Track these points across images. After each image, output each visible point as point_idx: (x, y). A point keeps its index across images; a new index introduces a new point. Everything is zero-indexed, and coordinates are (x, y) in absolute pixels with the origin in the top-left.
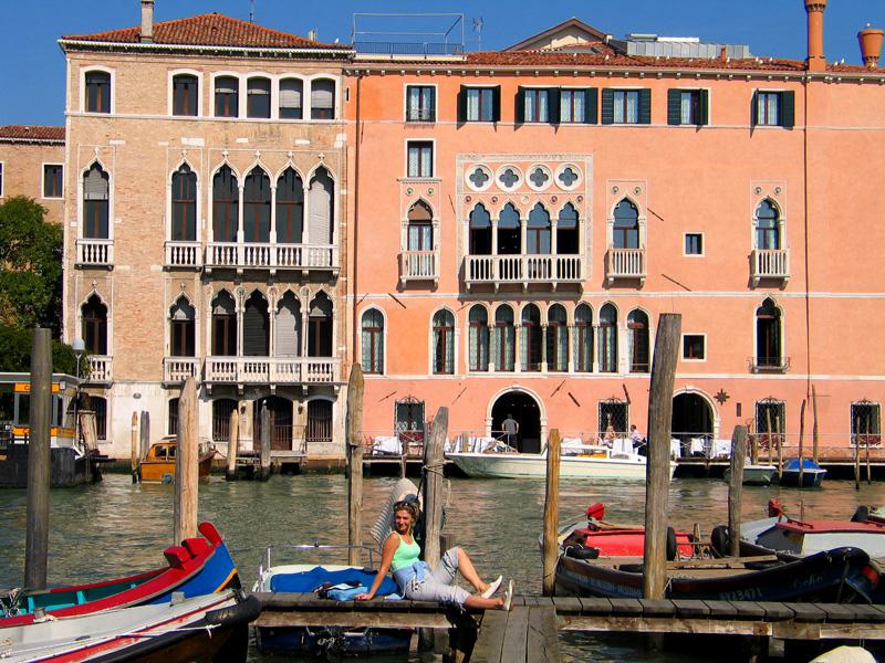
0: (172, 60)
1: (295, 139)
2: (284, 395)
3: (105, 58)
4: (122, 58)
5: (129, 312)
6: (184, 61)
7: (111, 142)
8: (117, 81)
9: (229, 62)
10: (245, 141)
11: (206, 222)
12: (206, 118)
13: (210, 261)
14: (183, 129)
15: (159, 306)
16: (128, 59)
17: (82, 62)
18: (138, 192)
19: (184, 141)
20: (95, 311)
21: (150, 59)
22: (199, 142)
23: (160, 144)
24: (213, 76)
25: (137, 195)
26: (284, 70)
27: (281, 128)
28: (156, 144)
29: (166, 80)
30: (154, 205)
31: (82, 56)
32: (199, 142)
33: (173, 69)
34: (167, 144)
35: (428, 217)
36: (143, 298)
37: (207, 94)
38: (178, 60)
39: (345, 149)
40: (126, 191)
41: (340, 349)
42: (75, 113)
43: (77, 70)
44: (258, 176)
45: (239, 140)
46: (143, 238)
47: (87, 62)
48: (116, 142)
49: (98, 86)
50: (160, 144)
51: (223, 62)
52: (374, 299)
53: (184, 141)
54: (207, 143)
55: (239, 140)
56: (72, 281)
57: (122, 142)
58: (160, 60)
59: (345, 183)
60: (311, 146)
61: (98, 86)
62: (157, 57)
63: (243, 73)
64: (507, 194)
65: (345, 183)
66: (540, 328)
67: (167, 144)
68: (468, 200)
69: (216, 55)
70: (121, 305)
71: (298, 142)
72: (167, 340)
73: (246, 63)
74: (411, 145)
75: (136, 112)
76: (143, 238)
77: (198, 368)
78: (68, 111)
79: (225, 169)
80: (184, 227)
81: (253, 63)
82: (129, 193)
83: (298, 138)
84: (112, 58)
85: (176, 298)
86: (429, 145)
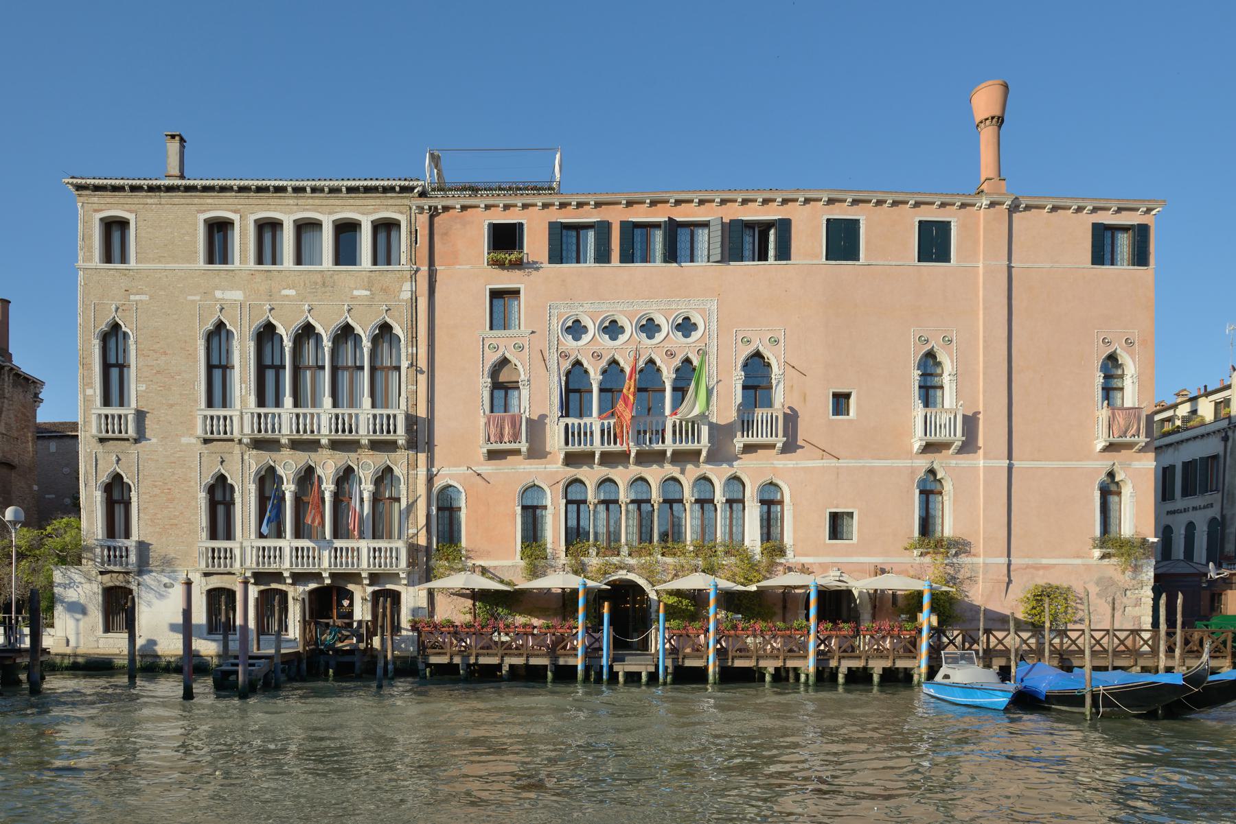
0: (202, 201)
1: (352, 289)
2: (340, 583)
3: (122, 201)
4: (142, 201)
5: (157, 491)
6: (216, 201)
7: (132, 297)
9: (271, 201)
10: (292, 292)
12: (243, 267)
13: (247, 430)
14: (217, 280)
15: (192, 483)
16: (149, 201)
17: (96, 207)
19: (218, 294)
20: (117, 494)
21: (176, 201)
22: (238, 295)
23: (190, 298)
25: (163, 358)
26: (338, 209)
27: (336, 277)
29: (196, 224)
31: (95, 199)
32: (238, 295)
34: (198, 298)
36: (174, 474)
37: (243, 240)
38: (209, 201)
39: (414, 300)
43: (91, 214)
44: (306, 332)
45: (285, 292)
46: (171, 406)
48: (138, 297)
49: (114, 229)
50: (190, 298)
51: (263, 201)
53: (218, 294)
54: (246, 294)
55: (285, 292)
57: (144, 297)
58: (188, 201)
60: (372, 298)
61: (114, 229)
62: (183, 197)
63: (288, 214)
65: (414, 339)
67: (198, 298)
71: (356, 293)
72: (203, 519)
73: (291, 202)
75: (160, 262)
76: (171, 406)
77: (237, 552)
78: (80, 263)
80: (217, 394)
81: (301, 202)
84: (129, 201)
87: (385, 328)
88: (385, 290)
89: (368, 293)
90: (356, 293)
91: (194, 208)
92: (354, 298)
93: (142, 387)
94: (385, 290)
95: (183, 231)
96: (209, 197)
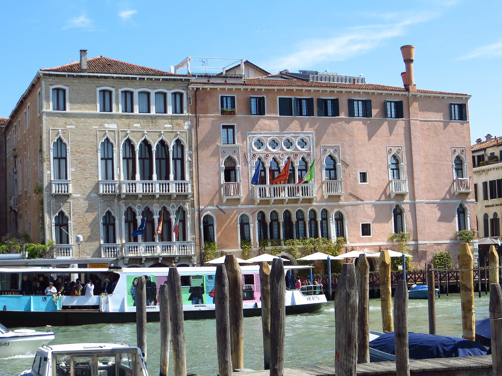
7: (68, 127)
8: (70, 93)
11: (120, 169)
16: (75, 81)
18: (82, 153)
23: (94, 127)
24: (120, 90)
25: (82, 156)
28: (92, 127)
30: (92, 161)
33: (99, 87)
34: (97, 127)
35: (233, 165)
39: (190, 130)
40: (77, 153)
41: (192, 236)
42: (48, 110)
44: (146, 144)
46: (87, 178)
47: (53, 83)
48: (70, 127)
50: (94, 127)
52: (209, 210)
53: (106, 125)
56: (49, 204)
59: (190, 147)
60: (173, 128)
64: (273, 153)
66: (291, 223)
67: (97, 127)
68: (254, 155)
69: (115, 79)
70: (76, 216)
71: (166, 126)
74: (224, 127)
76: (87, 178)
79: (129, 141)
82: (79, 154)
83: (166, 124)
84: (66, 81)
85: (105, 212)
86: (232, 127)
87: (178, 141)
88: (178, 124)
89: (171, 126)
90: (166, 126)
91: (95, 85)
92: (165, 128)
93: (73, 170)
94: (178, 124)
95: (90, 96)
96: (102, 81)
